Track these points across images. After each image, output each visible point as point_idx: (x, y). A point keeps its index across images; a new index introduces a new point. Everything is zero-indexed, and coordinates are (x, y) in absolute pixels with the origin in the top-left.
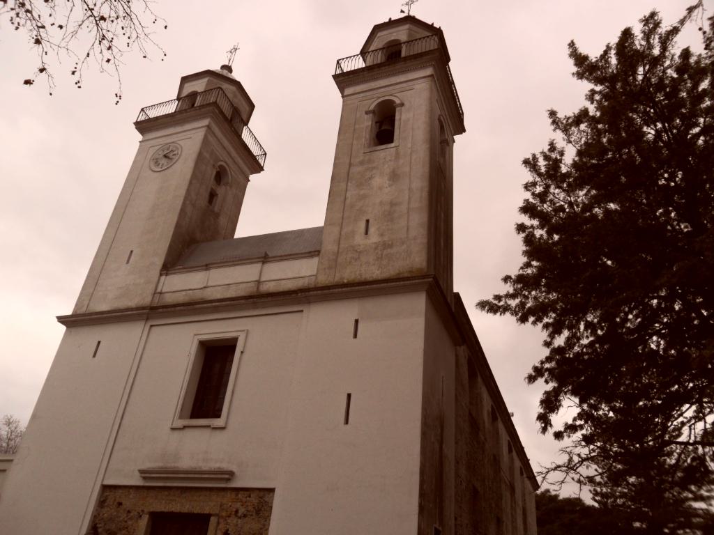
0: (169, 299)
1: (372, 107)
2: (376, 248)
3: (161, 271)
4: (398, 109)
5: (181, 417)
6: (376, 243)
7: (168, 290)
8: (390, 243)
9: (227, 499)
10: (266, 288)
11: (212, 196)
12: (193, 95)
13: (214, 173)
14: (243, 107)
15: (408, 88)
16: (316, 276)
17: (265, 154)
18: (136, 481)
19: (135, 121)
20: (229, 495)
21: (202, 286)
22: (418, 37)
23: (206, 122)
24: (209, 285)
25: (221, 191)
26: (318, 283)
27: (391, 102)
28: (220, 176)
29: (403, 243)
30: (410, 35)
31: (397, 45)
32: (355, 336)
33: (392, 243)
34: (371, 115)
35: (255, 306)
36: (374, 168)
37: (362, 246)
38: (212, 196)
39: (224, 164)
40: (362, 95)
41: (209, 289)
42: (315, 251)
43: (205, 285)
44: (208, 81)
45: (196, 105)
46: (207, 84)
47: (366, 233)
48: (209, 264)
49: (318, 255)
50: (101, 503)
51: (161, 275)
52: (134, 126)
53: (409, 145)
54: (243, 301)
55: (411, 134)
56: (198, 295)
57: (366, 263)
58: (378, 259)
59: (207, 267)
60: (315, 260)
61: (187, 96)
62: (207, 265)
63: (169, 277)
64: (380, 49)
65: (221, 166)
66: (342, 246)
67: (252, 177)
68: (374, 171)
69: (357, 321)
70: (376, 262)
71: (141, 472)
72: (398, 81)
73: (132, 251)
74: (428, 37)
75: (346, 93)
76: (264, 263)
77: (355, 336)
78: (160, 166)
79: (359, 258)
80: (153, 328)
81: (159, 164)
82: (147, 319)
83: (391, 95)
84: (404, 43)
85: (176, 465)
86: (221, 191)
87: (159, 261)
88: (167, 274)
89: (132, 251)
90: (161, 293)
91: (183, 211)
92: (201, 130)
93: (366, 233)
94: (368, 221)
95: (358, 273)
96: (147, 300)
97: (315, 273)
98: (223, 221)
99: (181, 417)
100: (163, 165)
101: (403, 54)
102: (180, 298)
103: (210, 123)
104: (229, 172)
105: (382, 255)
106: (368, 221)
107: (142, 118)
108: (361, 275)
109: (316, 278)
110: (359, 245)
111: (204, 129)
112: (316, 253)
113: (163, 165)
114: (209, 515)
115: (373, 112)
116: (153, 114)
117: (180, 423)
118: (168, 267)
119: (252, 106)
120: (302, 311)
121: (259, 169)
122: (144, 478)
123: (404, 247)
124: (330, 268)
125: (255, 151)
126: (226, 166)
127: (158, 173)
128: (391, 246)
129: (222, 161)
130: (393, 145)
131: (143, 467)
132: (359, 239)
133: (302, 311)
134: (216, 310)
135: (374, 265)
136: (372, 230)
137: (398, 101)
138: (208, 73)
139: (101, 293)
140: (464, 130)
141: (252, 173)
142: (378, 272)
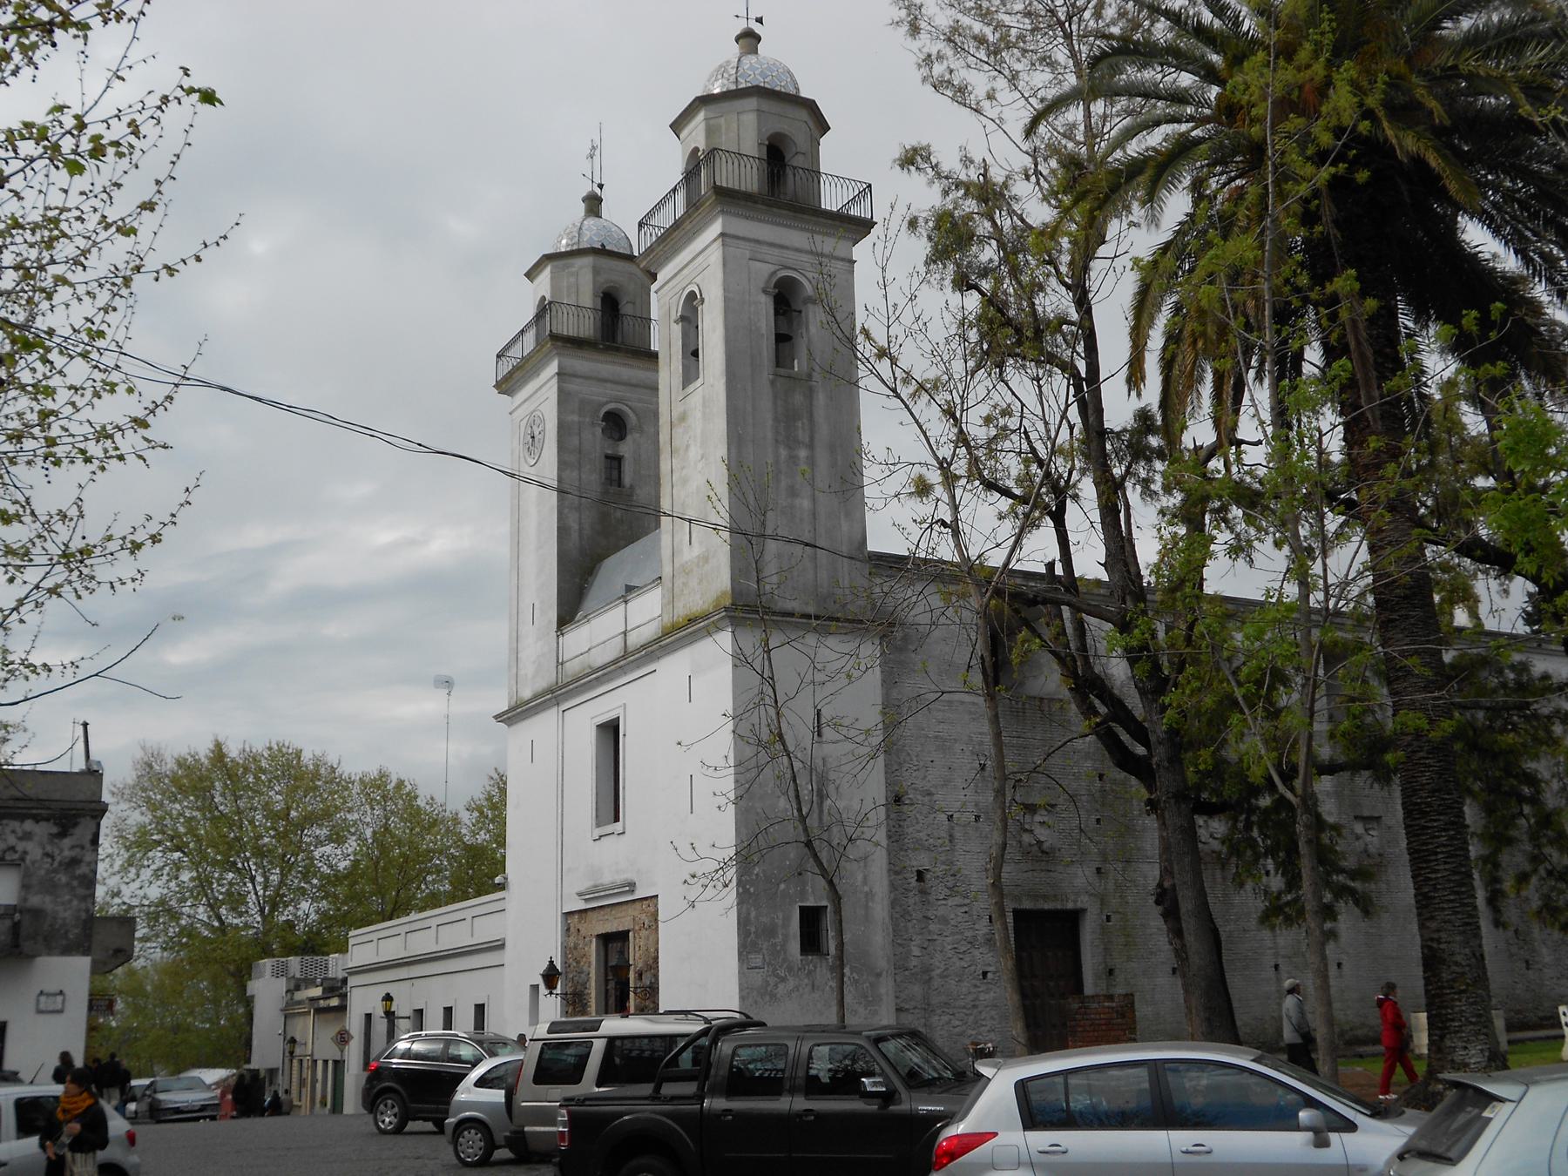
0: (573, 668)
2: (698, 565)
5: (598, 825)
9: (633, 911)
10: (635, 639)
11: (615, 461)
18: (581, 905)
20: (638, 905)
25: (625, 449)
28: (615, 424)
35: (623, 670)
40: (670, 284)
50: (567, 931)
71: (580, 894)
85: (600, 882)
86: (625, 449)
87: (553, 615)
91: (562, 531)
98: (642, 494)
99: (598, 825)
103: (560, 366)
104: (629, 411)
107: (506, 367)
111: (555, 380)
114: (628, 931)
117: (598, 832)
118: (569, 611)
122: (586, 900)
129: (607, 403)
131: (582, 889)
134: (599, 681)
138: (548, 258)
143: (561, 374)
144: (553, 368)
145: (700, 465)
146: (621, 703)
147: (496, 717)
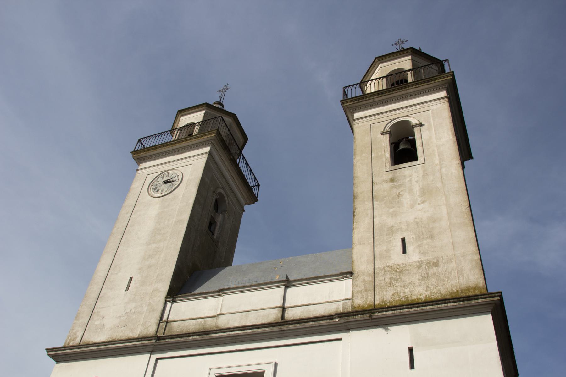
0: (176, 328)
1: (387, 129)
2: (419, 267)
3: (166, 298)
4: (416, 130)
6: (418, 262)
7: (176, 319)
8: (435, 261)
11: (212, 224)
12: (192, 125)
13: (214, 201)
14: (240, 140)
15: (423, 110)
16: (351, 299)
17: (259, 185)
19: (133, 150)
21: (215, 314)
22: (421, 65)
23: (207, 149)
24: (223, 312)
25: (219, 219)
26: (355, 307)
27: (408, 122)
28: (217, 205)
29: (450, 261)
30: (413, 64)
31: (401, 72)
32: (412, 366)
33: (438, 261)
34: (387, 136)
35: (282, 335)
36: (400, 186)
37: (402, 266)
38: (212, 224)
39: (223, 192)
40: (374, 118)
41: (221, 318)
42: (346, 273)
43: (219, 313)
44: (205, 112)
45: (193, 134)
46: (205, 116)
47: (404, 251)
48: (223, 290)
49: (351, 276)
51: (166, 302)
52: (131, 155)
53: (437, 162)
54: (267, 329)
55: (436, 151)
56: (210, 324)
57: (410, 283)
58: (423, 278)
59: (220, 292)
60: (347, 283)
61: (184, 126)
62: (219, 291)
63: (175, 305)
64: (383, 77)
65: (220, 194)
66: (376, 266)
67: (246, 207)
68: (401, 189)
69: (411, 350)
70: (423, 282)
72: (411, 104)
73: (131, 278)
74: (425, 66)
75: (355, 117)
76: (286, 287)
77: (412, 366)
78: (160, 191)
79: (400, 278)
80: (159, 361)
81: (158, 191)
82: (152, 352)
83: (407, 116)
84: (408, 71)
87: (165, 287)
88: (173, 301)
89: (131, 278)
90: (167, 322)
92: (204, 155)
93: (404, 251)
94: (403, 240)
95: (402, 294)
96: (151, 330)
97: (350, 296)
100: (162, 191)
101: (410, 80)
102: (192, 326)
103: (211, 150)
105: (427, 274)
106: (403, 240)
107: (139, 147)
108: (407, 298)
109: (353, 302)
110: (399, 265)
111: (207, 155)
112: (349, 275)
113: (162, 191)
115: (390, 133)
116: (148, 144)
119: (246, 139)
120: (341, 339)
121: (254, 199)
123: (453, 264)
124: (366, 290)
125: (251, 183)
126: (225, 195)
127: (158, 198)
128: (436, 265)
130: (417, 162)
132: (397, 258)
133: (341, 339)
134: (235, 340)
135: (420, 285)
136: (409, 248)
137: (414, 121)
138: (207, 106)
139: (96, 323)
140: (472, 158)
141: (247, 204)
142: (428, 293)
143: (210, 153)
144: (207, 149)
145: (420, 207)
146: (273, 360)
147: (49, 350)
